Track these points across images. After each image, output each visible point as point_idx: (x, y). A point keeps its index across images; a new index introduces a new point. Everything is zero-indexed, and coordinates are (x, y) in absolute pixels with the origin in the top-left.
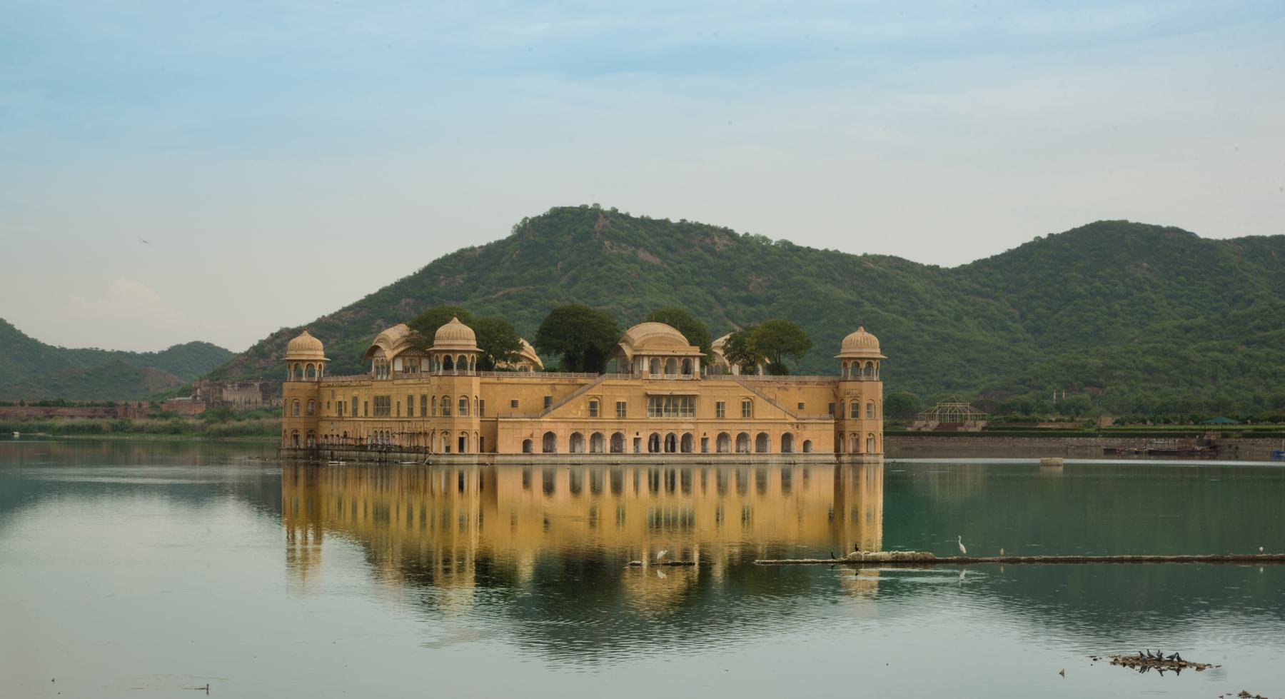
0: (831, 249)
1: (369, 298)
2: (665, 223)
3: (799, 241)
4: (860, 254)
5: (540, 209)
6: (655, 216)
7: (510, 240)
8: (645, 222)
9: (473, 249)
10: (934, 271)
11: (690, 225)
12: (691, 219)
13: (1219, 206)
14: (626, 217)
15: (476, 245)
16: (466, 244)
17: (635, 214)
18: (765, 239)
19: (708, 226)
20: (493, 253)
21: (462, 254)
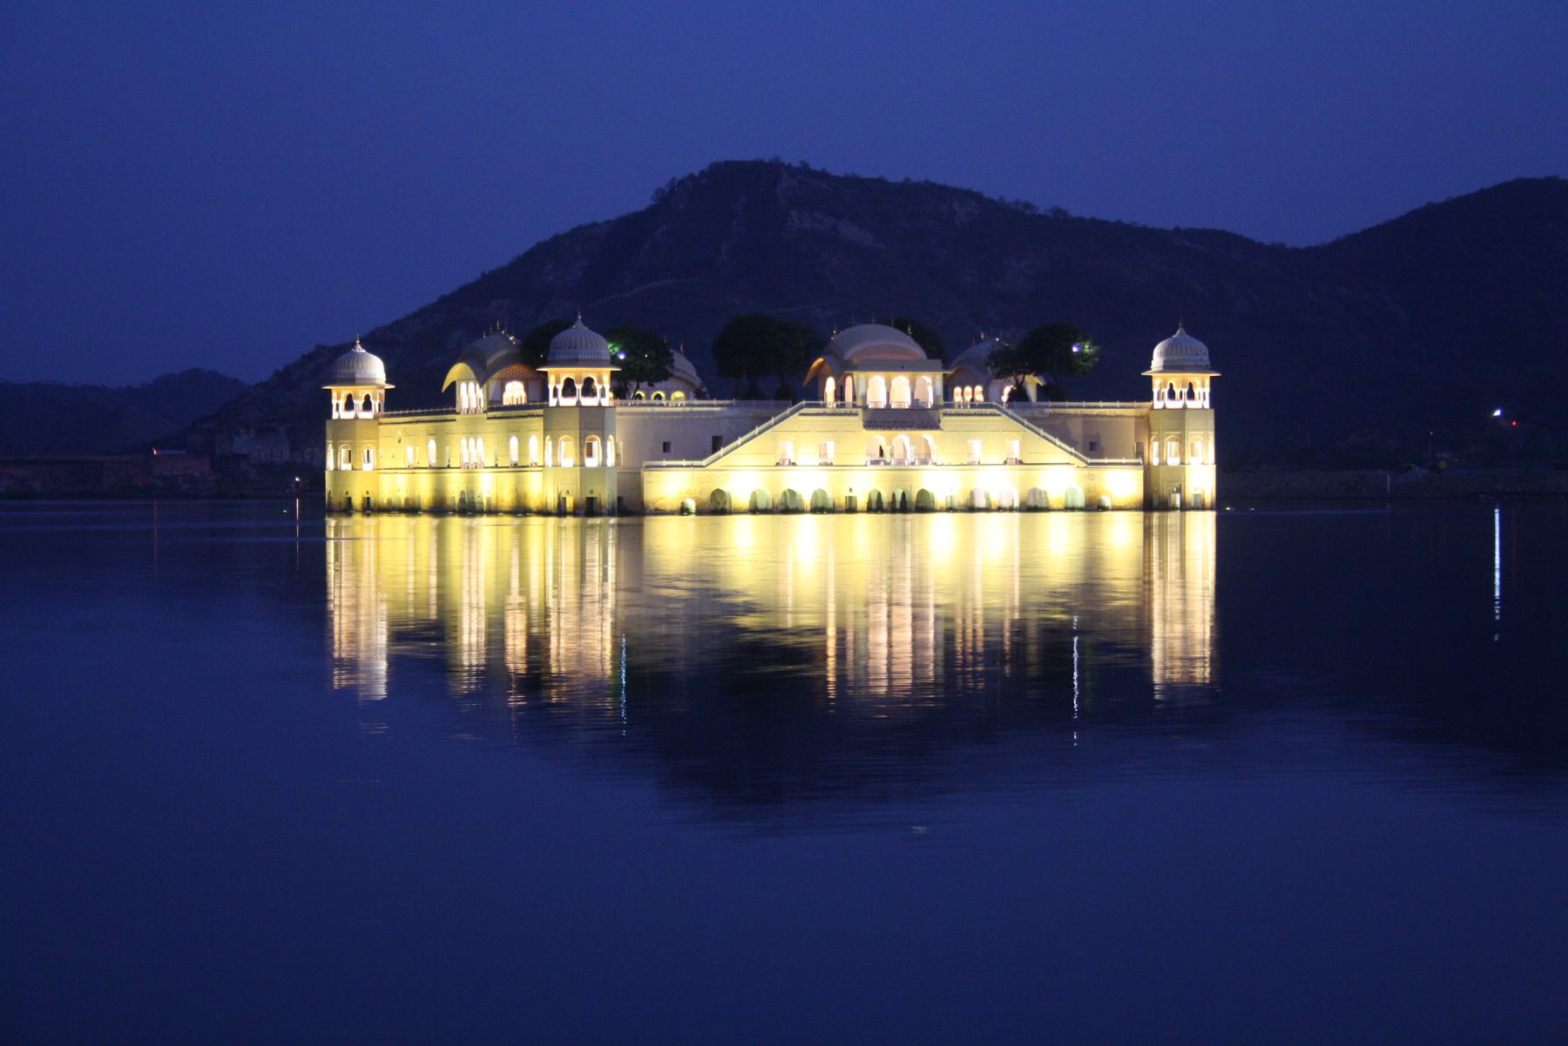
0: (1127, 220)
1: (444, 300)
2: (881, 182)
3: (1078, 209)
4: (1169, 227)
5: (697, 164)
6: (866, 173)
7: (651, 212)
8: (853, 182)
9: (594, 225)
10: (1277, 252)
11: (915, 185)
12: (918, 176)
13: (1567, 170)
14: (824, 176)
15: (600, 220)
16: (586, 220)
17: (838, 171)
18: (1028, 205)
19: (944, 189)
20: (630, 228)
21: (579, 234)
